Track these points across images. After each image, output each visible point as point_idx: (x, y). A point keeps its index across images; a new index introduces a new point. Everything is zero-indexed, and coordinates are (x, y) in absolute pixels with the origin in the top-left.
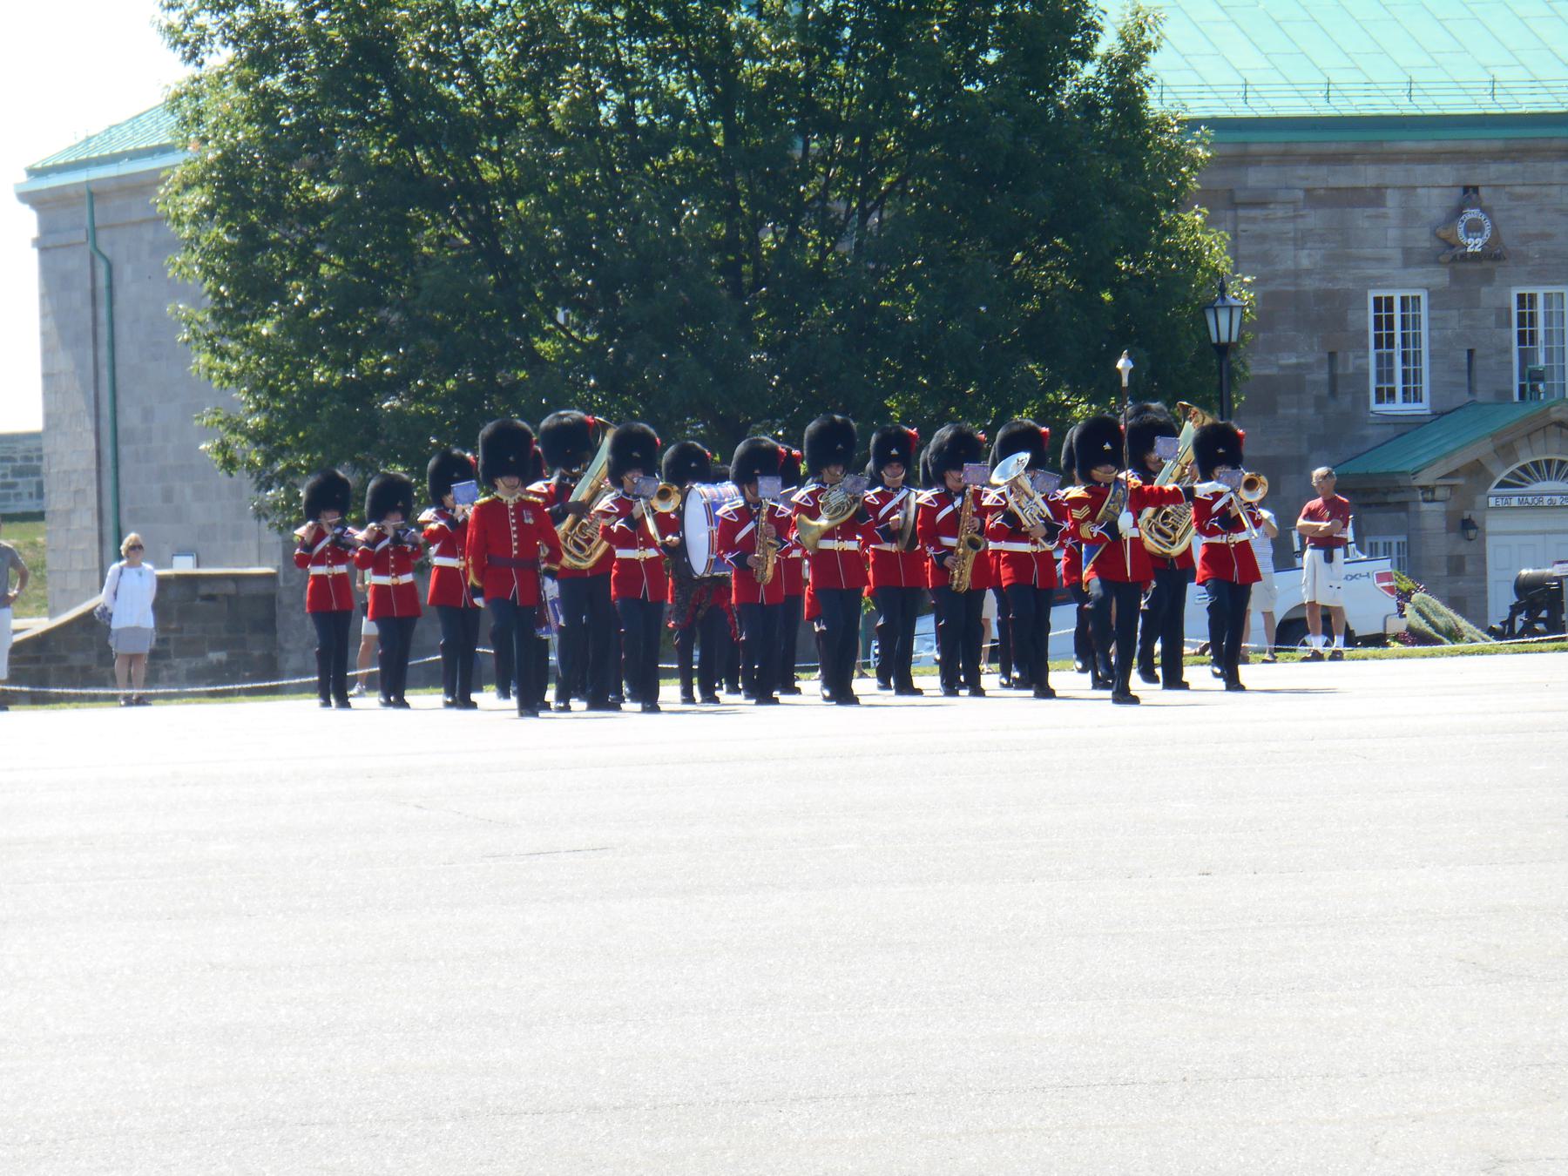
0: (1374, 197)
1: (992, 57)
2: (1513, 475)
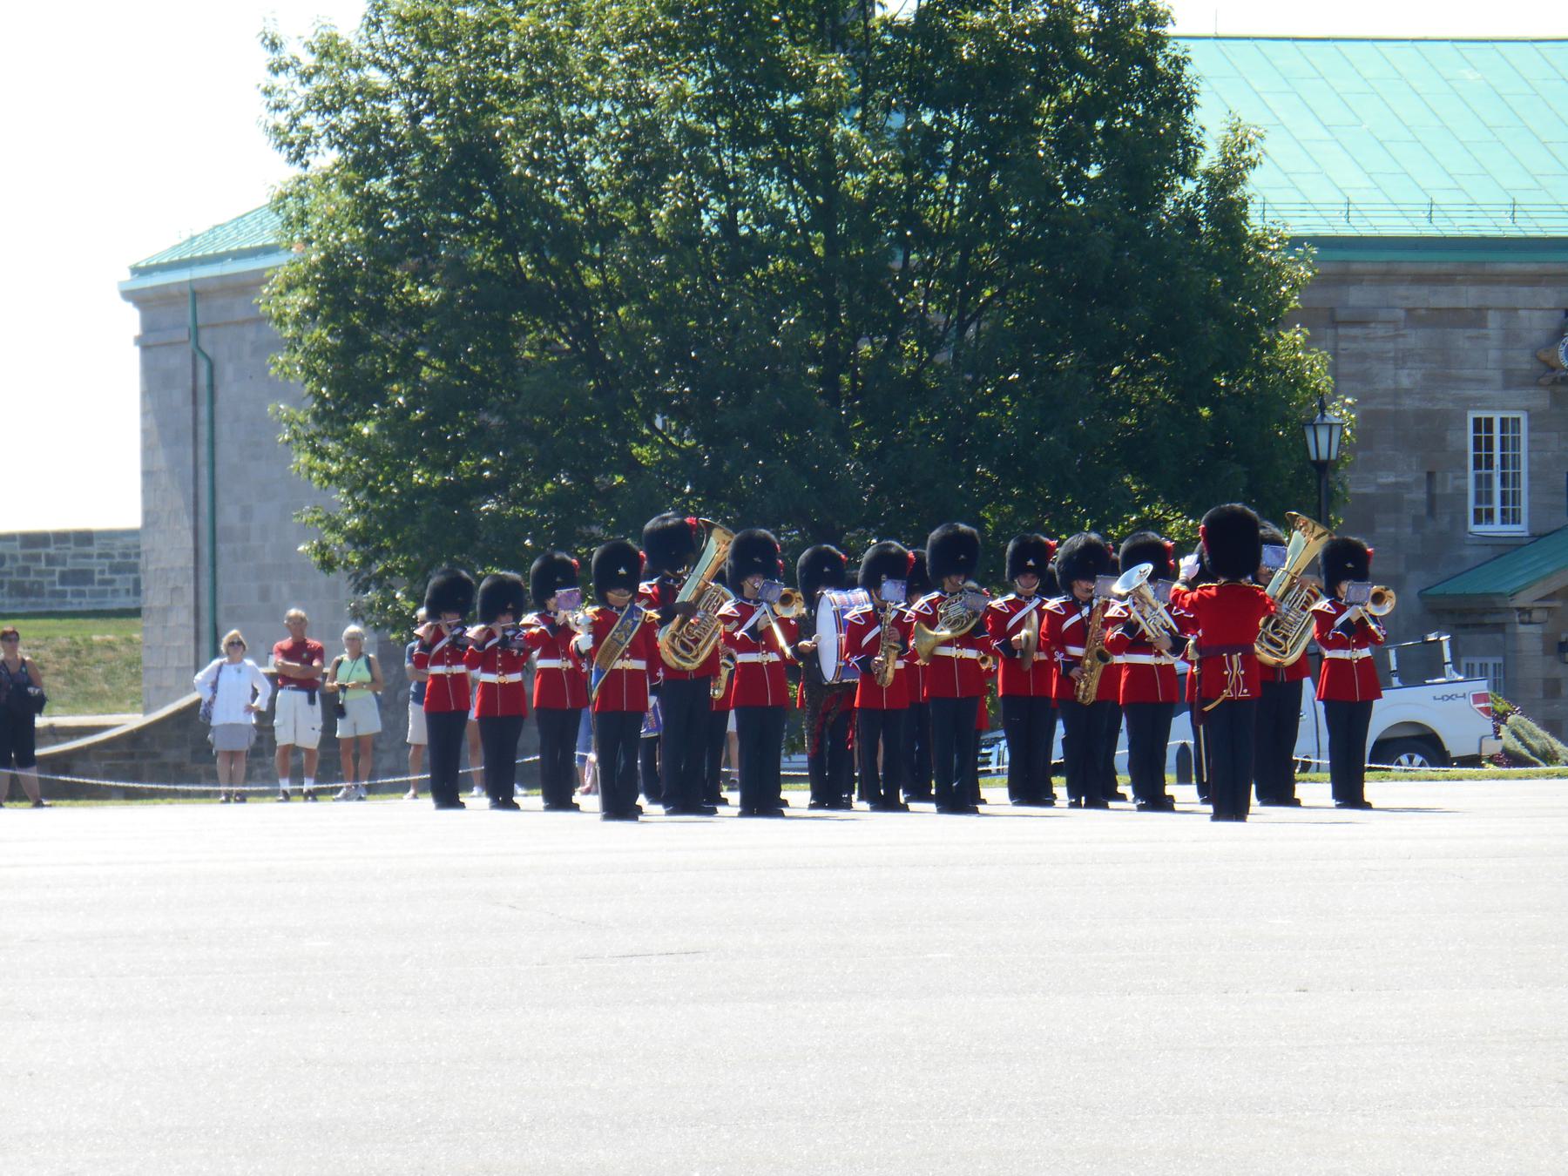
0: (1474, 318)
1: (1093, 172)
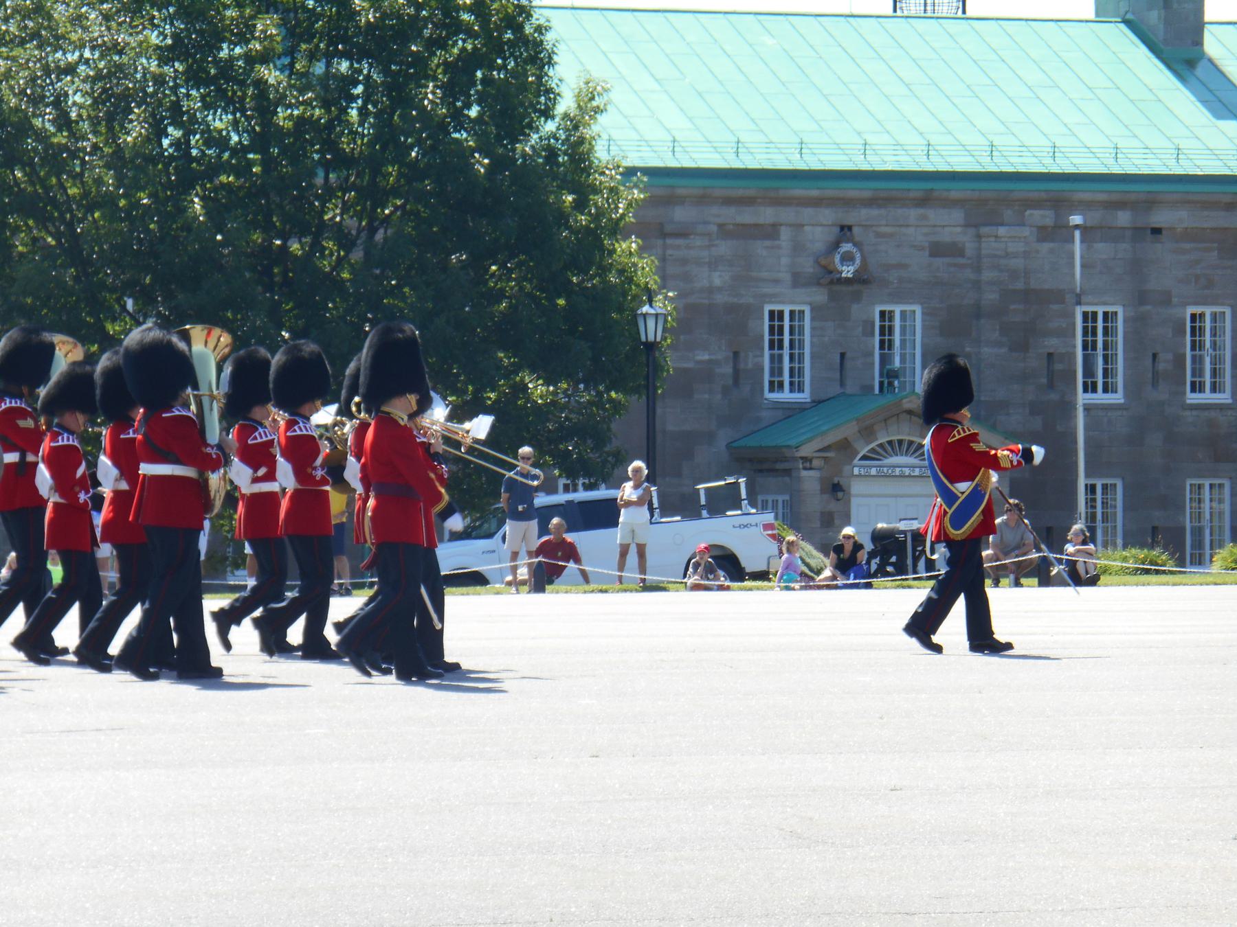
0: (770, 232)
1: (474, 112)
2: (873, 451)
